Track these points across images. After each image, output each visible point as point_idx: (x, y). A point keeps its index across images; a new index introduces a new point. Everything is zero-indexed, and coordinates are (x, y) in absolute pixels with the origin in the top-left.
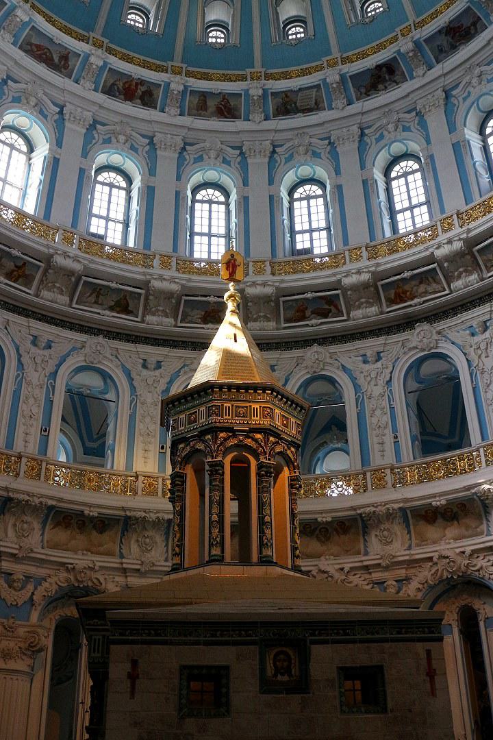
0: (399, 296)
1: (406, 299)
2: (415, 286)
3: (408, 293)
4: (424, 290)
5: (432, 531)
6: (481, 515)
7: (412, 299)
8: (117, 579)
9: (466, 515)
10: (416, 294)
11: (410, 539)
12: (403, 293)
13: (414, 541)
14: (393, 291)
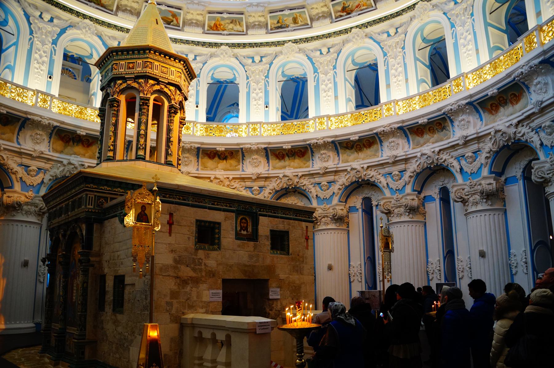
0: (216, 26)
1: (220, 29)
2: (228, 23)
3: (222, 26)
4: (232, 28)
5: (210, 163)
6: (239, 160)
7: (223, 31)
8: (15, 158)
9: (231, 158)
10: (226, 28)
11: (198, 165)
12: (219, 25)
13: (200, 167)
14: (214, 22)
